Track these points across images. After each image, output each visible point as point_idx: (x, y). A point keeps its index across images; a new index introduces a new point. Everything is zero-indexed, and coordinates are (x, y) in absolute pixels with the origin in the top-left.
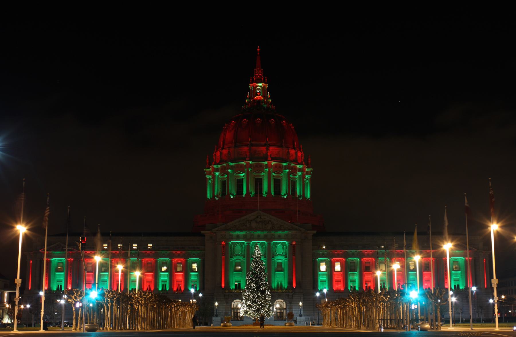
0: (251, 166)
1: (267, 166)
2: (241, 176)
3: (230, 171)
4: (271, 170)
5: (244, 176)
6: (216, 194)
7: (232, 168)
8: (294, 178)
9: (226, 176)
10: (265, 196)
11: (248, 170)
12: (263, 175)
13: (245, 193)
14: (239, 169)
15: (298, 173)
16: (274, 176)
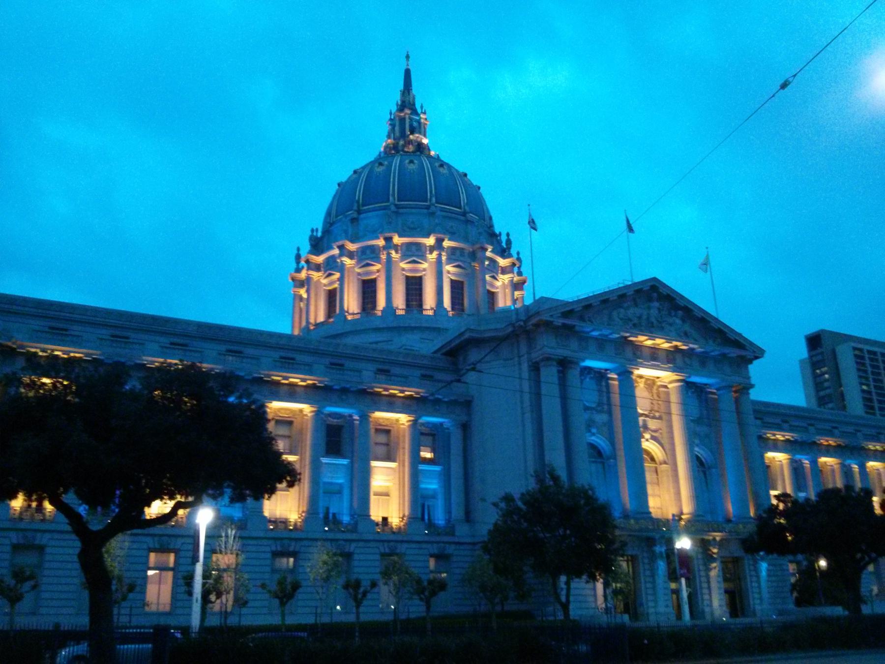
0: (396, 248)
1: (432, 249)
2: (371, 273)
3: (347, 261)
4: (444, 258)
5: (378, 271)
6: (312, 320)
7: (351, 255)
8: (493, 286)
9: (337, 275)
10: (431, 313)
11: (389, 254)
12: (424, 270)
13: (381, 303)
14: (368, 255)
15: (501, 276)
16: (449, 272)
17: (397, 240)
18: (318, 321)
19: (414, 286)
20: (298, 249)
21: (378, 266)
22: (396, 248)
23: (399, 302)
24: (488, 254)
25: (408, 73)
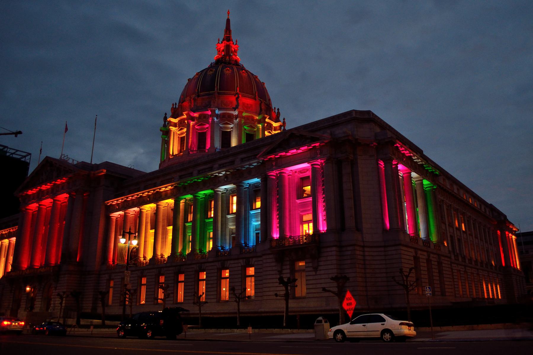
0: (217, 116)
5: (207, 128)
9: (185, 130)
11: (213, 120)
12: (232, 128)
13: (208, 146)
16: (245, 129)
17: (217, 112)
18: (175, 154)
19: (226, 137)
20: (166, 114)
21: (207, 126)
22: (217, 116)
23: (218, 144)
24: (267, 120)
25: (228, 21)
